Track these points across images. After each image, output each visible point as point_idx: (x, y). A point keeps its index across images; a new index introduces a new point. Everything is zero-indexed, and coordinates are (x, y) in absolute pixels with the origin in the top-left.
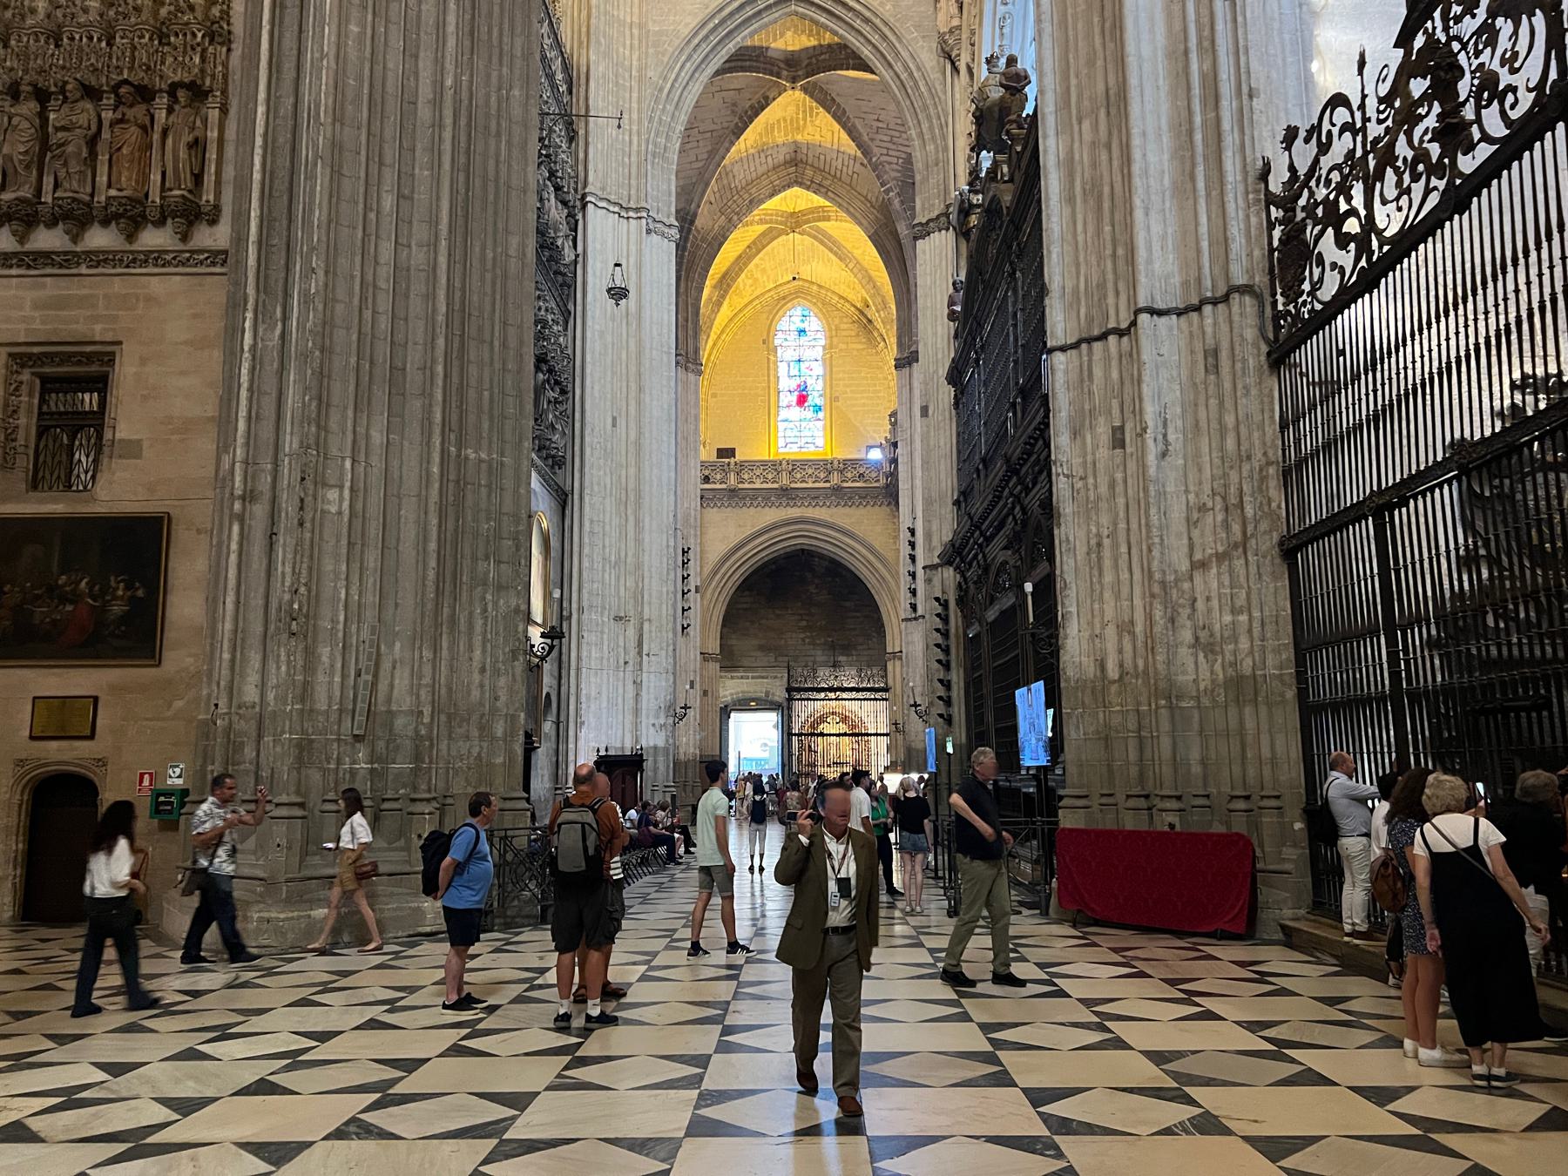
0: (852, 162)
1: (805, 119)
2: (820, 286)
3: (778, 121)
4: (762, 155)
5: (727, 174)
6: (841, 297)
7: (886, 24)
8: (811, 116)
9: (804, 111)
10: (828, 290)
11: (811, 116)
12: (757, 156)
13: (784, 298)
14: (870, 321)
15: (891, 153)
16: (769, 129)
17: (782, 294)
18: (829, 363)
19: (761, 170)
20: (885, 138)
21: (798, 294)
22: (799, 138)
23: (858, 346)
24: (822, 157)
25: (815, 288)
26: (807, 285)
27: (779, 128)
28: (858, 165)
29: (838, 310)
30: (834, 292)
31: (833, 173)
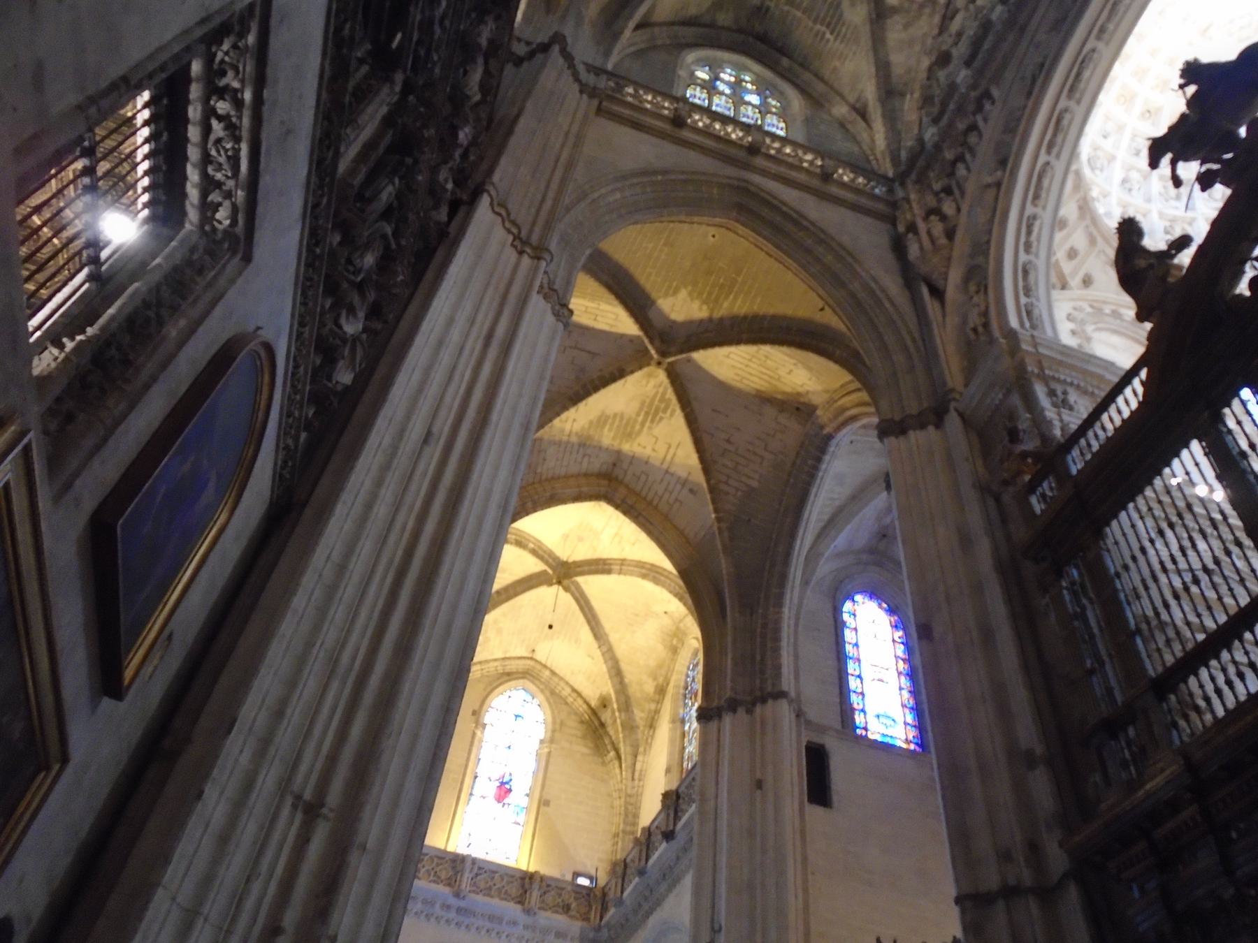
0: (679, 487)
1: (643, 424)
2: (553, 673)
3: (615, 415)
4: (581, 450)
5: (539, 451)
6: (574, 690)
7: (844, 249)
8: (652, 421)
9: (647, 414)
10: (561, 679)
11: (652, 421)
12: (576, 447)
13: (509, 674)
14: (602, 725)
15: (731, 482)
16: (602, 420)
17: (508, 669)
18: (546, 763)
19: (574, 469)
20: (729, 464)
21: (525, 674)
22: (626, 447)
23: (582, 749)
24: (643, 478)
25: (547, 673)
26: (539, 667)
27: (612, 424)
28: (685, 491)
29: (566, 703)
30: (567, 683)
31: (649, 498)
